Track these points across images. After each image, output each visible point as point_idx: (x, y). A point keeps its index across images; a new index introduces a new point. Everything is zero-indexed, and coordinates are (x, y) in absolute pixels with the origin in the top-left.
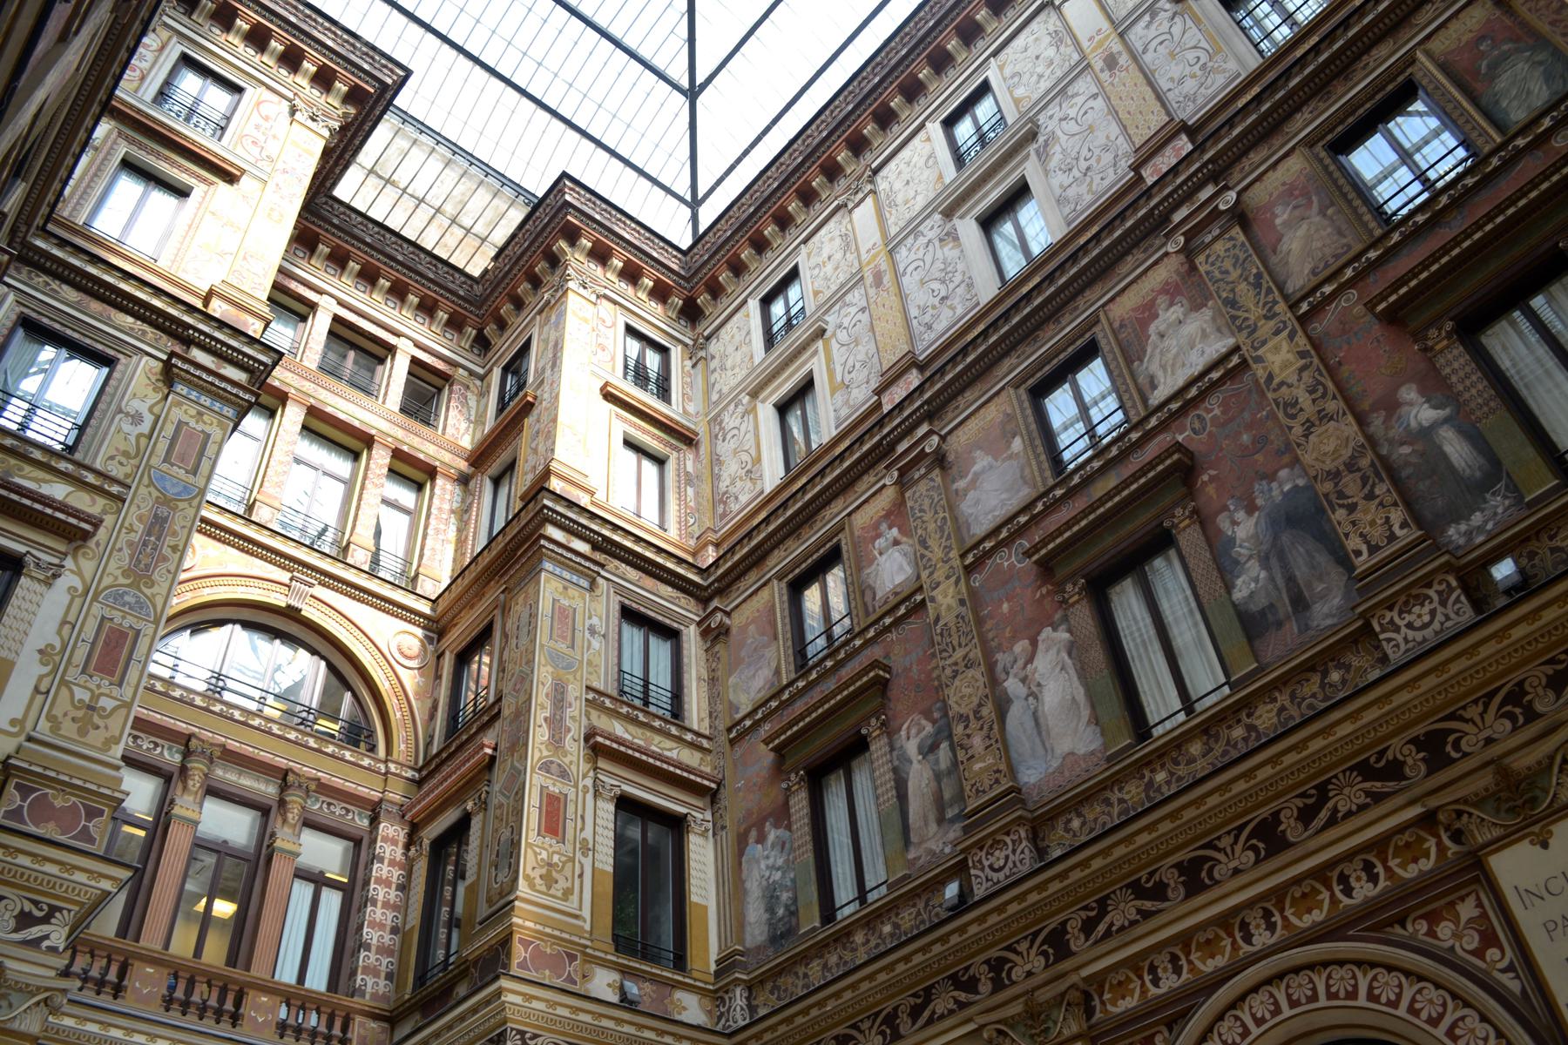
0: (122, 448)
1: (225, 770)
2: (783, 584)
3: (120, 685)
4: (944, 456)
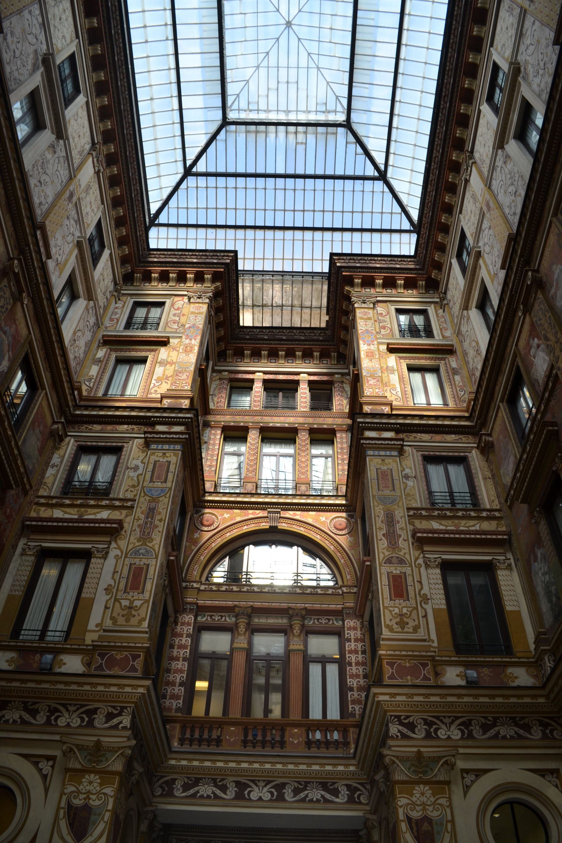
0: (131, 484)
1: (259, 617)
2: (505, 404)
3: (143, 593)
4: (541, 281)
